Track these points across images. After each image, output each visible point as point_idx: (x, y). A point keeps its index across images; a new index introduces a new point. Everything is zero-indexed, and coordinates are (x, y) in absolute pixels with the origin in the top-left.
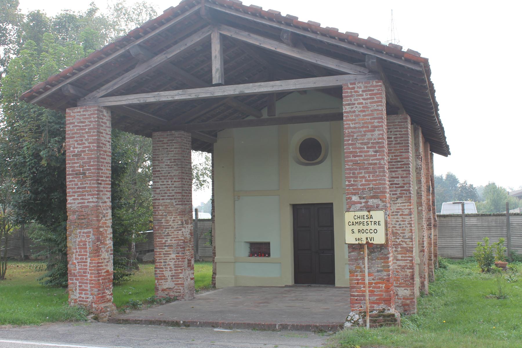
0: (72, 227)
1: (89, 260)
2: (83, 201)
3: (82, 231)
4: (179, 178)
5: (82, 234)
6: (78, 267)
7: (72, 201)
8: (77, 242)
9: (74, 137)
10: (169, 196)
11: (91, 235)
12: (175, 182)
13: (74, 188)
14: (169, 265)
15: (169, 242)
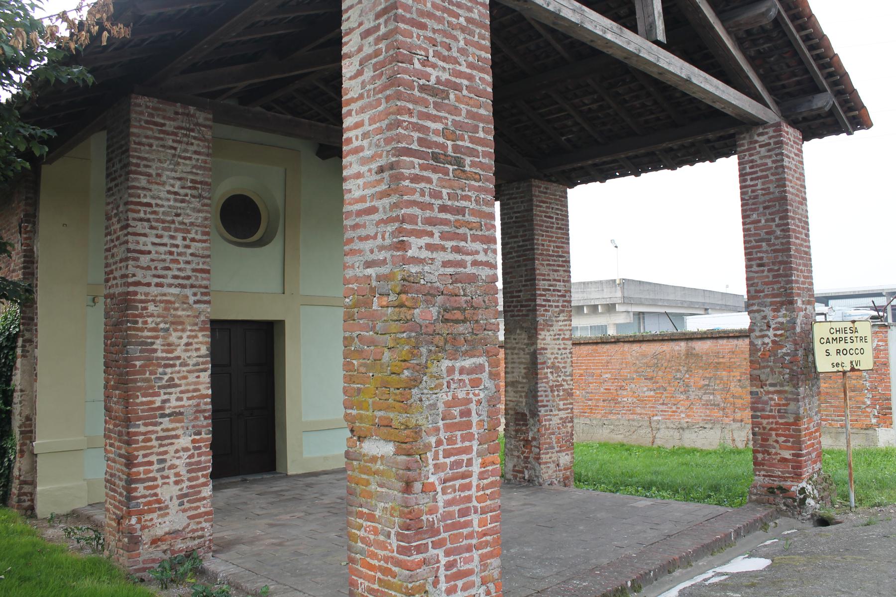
0: (424, 350)
1: (476, 469)
2: (458, 257)
3: (458, 364)
4: (205, 233)
5: (457, 376)
6: (441, 499)
7: (425, 254)
8: (441, 407)
9: (423, 27)
10: (175, 277)
11: (485, 376)
12: (193, 240)
13: (430, 206)
14: (172, 467)
15: (174, 403)
